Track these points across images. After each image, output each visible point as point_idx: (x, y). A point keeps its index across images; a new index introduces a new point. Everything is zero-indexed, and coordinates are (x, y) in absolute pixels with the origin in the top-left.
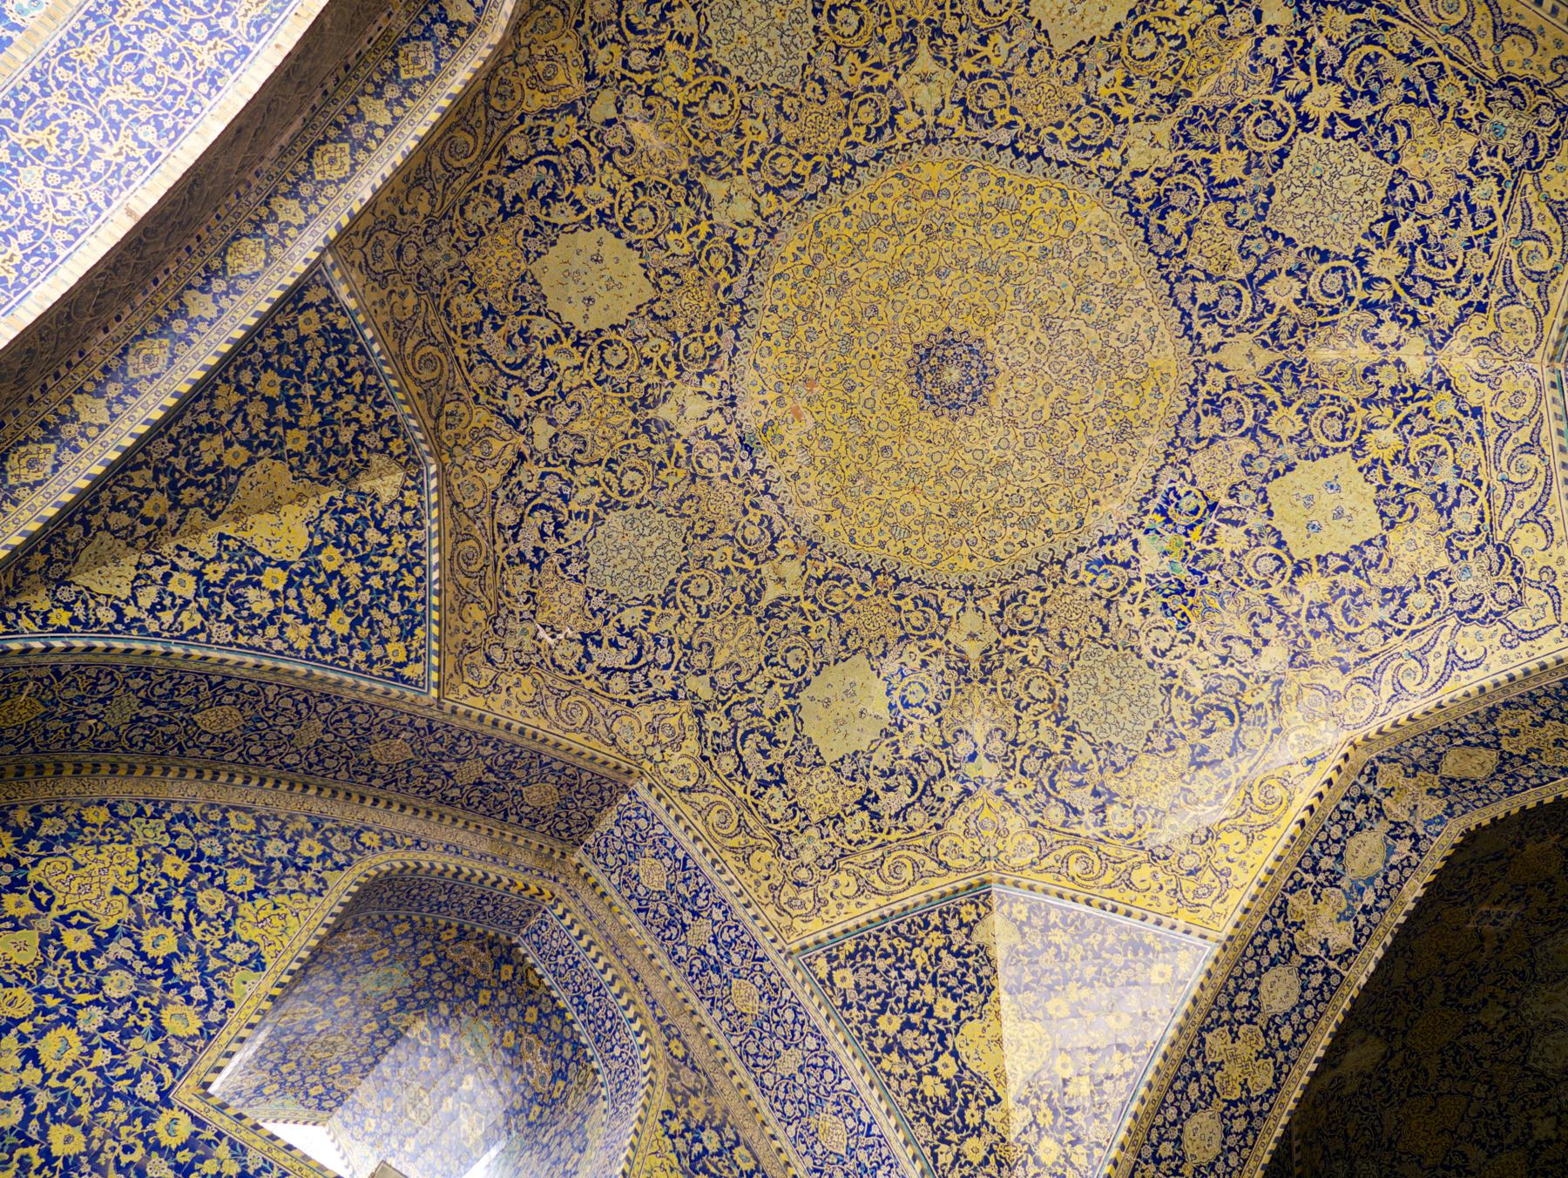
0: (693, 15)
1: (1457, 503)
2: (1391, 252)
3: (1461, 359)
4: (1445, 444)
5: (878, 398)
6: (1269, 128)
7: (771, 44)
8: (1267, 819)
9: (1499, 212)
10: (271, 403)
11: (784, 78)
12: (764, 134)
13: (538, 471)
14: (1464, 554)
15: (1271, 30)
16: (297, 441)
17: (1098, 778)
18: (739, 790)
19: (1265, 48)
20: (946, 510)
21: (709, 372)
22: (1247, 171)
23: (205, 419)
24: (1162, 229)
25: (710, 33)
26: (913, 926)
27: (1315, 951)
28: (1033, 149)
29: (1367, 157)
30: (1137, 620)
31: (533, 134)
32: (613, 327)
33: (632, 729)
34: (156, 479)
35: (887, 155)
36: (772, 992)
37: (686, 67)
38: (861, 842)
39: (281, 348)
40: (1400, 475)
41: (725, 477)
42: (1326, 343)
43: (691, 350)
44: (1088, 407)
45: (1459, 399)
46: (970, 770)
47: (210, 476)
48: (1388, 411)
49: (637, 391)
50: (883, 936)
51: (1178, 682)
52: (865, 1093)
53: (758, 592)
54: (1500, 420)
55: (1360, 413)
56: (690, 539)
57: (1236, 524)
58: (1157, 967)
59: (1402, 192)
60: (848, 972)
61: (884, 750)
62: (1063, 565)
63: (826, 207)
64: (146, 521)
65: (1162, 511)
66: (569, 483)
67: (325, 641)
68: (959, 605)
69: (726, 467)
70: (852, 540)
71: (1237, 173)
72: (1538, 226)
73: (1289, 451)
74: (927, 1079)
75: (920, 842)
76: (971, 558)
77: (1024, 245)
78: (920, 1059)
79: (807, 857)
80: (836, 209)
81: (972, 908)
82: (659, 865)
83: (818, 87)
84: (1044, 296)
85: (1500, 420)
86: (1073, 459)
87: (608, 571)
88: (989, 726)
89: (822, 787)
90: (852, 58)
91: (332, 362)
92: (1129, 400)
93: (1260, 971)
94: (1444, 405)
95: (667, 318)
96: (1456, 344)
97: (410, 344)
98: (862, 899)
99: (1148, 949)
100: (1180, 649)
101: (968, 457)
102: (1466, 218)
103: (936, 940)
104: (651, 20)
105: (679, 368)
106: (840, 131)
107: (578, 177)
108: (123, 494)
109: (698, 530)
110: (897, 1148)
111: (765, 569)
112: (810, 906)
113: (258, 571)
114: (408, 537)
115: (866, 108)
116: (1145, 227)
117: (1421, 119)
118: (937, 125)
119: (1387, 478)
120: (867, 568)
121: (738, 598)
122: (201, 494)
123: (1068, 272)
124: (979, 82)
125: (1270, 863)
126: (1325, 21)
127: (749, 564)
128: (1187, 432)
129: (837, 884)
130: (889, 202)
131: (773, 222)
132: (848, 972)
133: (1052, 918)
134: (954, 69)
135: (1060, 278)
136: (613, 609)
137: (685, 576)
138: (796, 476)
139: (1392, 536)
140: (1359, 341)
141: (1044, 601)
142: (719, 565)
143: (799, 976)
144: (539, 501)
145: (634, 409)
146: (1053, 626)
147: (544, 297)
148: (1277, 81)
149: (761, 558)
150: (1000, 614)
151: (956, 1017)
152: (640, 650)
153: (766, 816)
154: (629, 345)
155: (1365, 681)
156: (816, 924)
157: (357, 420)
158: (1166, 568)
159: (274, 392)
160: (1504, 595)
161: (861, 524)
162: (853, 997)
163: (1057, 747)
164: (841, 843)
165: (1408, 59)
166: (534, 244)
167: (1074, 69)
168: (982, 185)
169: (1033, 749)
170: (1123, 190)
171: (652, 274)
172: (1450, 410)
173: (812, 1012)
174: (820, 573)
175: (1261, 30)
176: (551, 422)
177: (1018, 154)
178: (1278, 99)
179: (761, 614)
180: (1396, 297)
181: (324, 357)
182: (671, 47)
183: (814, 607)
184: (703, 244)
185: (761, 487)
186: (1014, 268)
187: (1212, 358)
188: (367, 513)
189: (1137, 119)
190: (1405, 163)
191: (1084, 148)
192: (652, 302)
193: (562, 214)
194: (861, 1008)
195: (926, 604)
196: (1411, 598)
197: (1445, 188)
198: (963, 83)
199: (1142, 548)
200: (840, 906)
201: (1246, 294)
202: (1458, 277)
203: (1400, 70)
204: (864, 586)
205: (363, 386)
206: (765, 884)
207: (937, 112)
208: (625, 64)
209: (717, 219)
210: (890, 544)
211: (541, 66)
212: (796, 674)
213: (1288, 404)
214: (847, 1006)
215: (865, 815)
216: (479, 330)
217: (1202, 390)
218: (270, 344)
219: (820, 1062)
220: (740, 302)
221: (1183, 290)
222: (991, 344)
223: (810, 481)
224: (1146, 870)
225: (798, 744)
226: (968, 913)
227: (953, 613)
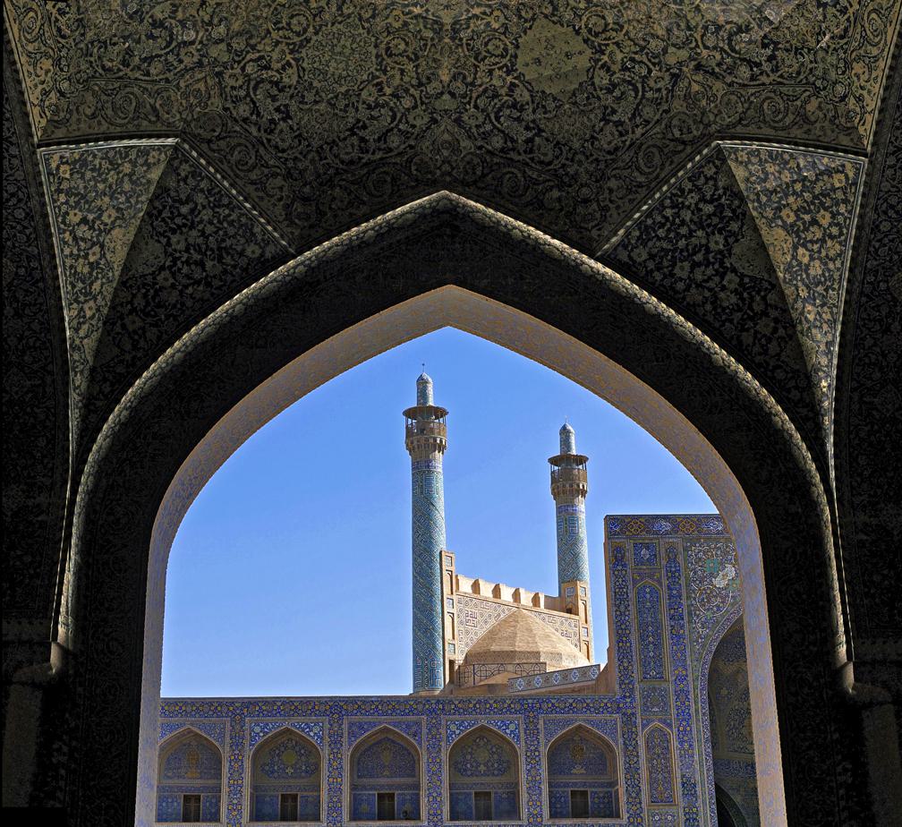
0: (363, 93)
7: (344, 47)
10: (695, 265)
13: (705, 53)
16: (718, 242)
23: (708, 307)
25: (365, 77)
31: (485, 136)
32: (578, 32)
34: (748, 330)
37: (393, 76)
39: (658, 269)
47: (745, 295)
64: (775, 330)
67: (835, 231)
91: (661, 233)
97: (642, 179)
104: (383, 111)
107: (496, 96)
108: (757, 349)
113: (800, 264)
122: (758, 298)
144: (726, 47)
154: (584, 18)
157: (696, 204)
159: (686, 265)
166: (551, 105)
171: (528, 25)
176: (665, 51)
181: (659, 239)
182: (388, 91)
192: (546, 16)
193: (523, 95)
205: (672, 208)
208: (415, 107)
211: (446, 153)
216: (619, 123)
218: (658, 276)
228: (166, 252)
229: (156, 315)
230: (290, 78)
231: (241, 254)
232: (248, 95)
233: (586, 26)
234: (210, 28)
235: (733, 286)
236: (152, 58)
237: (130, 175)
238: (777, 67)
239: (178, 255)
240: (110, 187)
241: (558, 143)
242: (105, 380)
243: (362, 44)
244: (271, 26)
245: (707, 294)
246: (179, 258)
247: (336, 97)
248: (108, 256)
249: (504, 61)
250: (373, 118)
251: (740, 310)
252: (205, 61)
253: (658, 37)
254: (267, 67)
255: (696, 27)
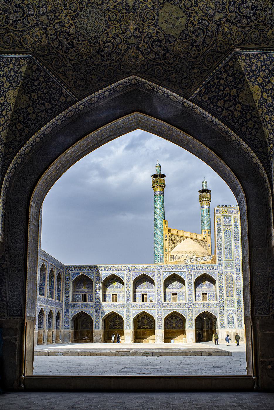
7: (92, 17)
10: (225, 102)
11: (96, 8)
13: (230, 14)
16: (234, 92)
23: (230, 117)
25: (101, 30)
31: (148, 54)
32: (181, 8)
34: (244, 126)
39: (212, 103)
47: (244, 112)
64: (254, 125)
91: (213, 89)
97: (205, 68)
104: (109, 44)
107: (151, 37)
108: (248, 133)
113: (264, 99)
122: (248, 114)
147: (183, 31)
157: (226, 77)
166: (172, 39)
171: (162, 5)
176: (214, 14)
181: (212, 92)
182: (111, 36)
188: (249, 69)
193: (161, 36)
205: (217, 79)
208: (121, 42)
211: (134, 61)
216: (197, 46)
218: (212, 106)
228: (30, 100)
229: (28, 123)
230: (73, 30)
231: (58, 100)
232: (57, 37)
233: (184, 5)
234: (39, 8)
235: (239, 109)
236: (17, 21)
237: (13, 69)
238: (257, 18)
239: (34, 101)
240: (6, 73)
241: (175, 55)
242: (10, 147)
243: (99, 16)
244: (63, 8)
245: (230, 112)
246: (35, 102)
247: (91, 38)
248: (8, 101)
249: (154, 22)
250: (105, 47)
251: (241, 118)
252: (39, 23)
253: (211, 9)
254: (63, 26)
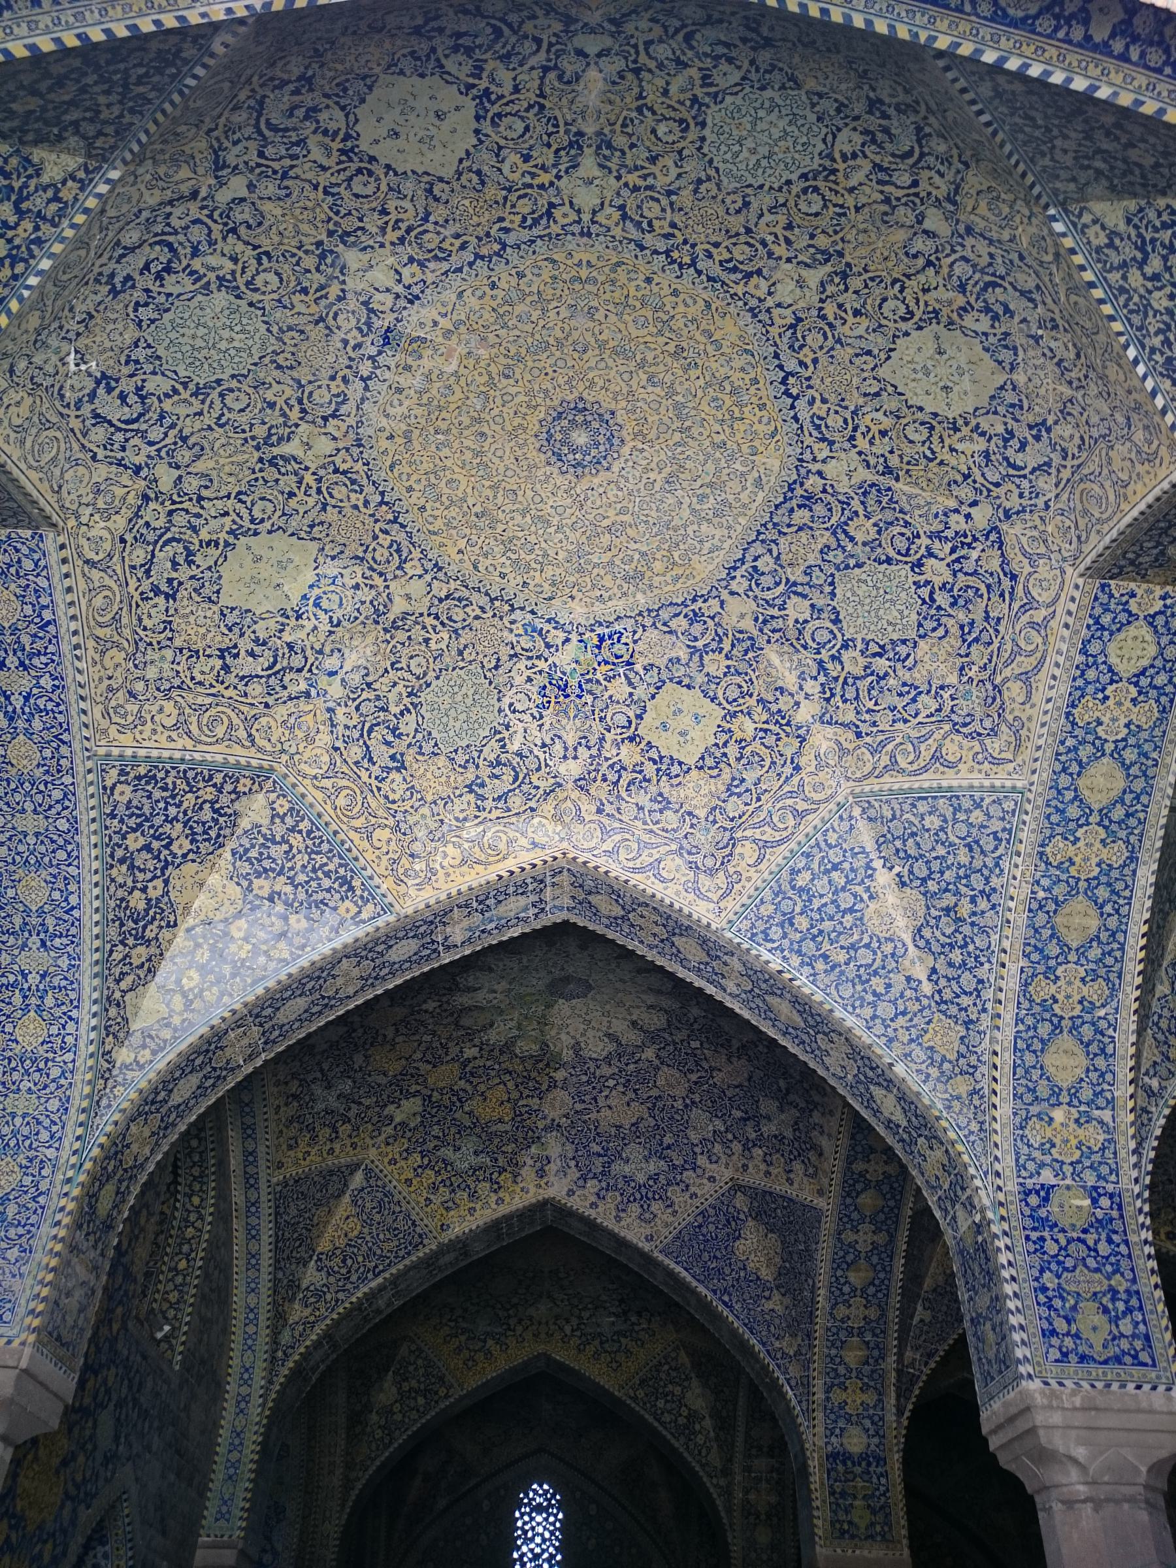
1: (739, 795)
2: (862, 661)
3: (822, 739)
4: (767, 763)
5: (517, 400)
6: (902, 544)
7: (753, 151)
8: (483, 858)
9: (920, 719)
12: (668, 180)
14: (715, 822)
15: (968, 516)
17: (403, 749)
18: (133, 583)
19: (954, 517)
20: (478, 509)
21: (421, 264)
22: (865, 544)
24: (792, 510)
26: (195, 776)
27: (440, 939)
28: (794, 391)
29: (914, 617)
30: (519, 680)
33: (80, 482)
35: (718, 285)
36: (55, 769)
37: (682, 91)
38: (200, 683)
40: (732, 751)
41: (345, 342)
42: (781, 654)
43: (426, 237)
44: (633, 546)
45: (798, 753)
46: (323, 681)
48: (765, 717)
49: (349, 224)
50: (173, 773)
51: (506, 734)
52: (85, 886)
53: (280, 439)
54: (801, 785)
55: (752, 702)
56: (267, 360)
57: (630, 684)
58: (347, 903)
59: (903, 650)
60: (128, 789)
61: (272, 624)
62: (513, 609)
63: (640, 261)
65: (601, 639)
66: (212, 243)
68: (420, 571)
69: (354, 337)
70: (392, 467)
71: (860, 537)
72: (923, 747)
73: (700, 679)
74: (137, 893)
75: (245, 709)
76: (460, 552)
77: (717, 427)
78: (140, 876)
79: (151, 673)
80: (644, 270)
81: (248, 782)
82: (17, 604)
83: (740, 204)
84: (689, 464)
85: (801, 785)
86: (589, 562)
87: (173, 335)
88: (362, 662)
89: (201, 621)
90: (783, 220)
92: (658, 566)
93: (406, 937)
94: (789, 747)
95: (437, 200)
96: (830, 731)
98: (174, 735)
99: (351, 889)
100: (527, 717)
101: (530, 493)
102: (907, 698)
103: (208, 793)
104: (708, 50)
105: (402, 240)
106: (714, 239)
109: (280, 360)
110: (86, 935)
111: (304, 426)
112: (130, 719)
114: (37, 228)
115: (747, 249)
116: (785, 500)
117: (954, 641)
118: (768, 311)
119: (725, 744)
120: (382, 494)
121: (260, 431)
123: (718, 471)
124: (822, 324)
125: (464, 888)
126: (989, 552)
127: (295, 415)
128: (665, 615)
129: (161, 710)
130: (681, 308)
131: (594, 229)
132: (128, 789)
133: (302, 826)
134: (822, 301)
135: (710, 467)
136: (148, 368)
137: (234, 384)
138: (399, 391)
139: (694, 773)
140: (796, 673)
141: (477, 618)
142: (269, 396)
143: (90, 777)
145: (330, 234)
146: (466, 637)
148: (936, 535)
149: (309, 418)
150: (441, 600)
151: (184, 856)
152: (141, 415)
153: (140, 620)
154: (384, 188)
155: (603, 828)
156: (126, 739)
158: (568, 669)
160: (709, 862)
161: (410, 463)
162: (121, 810)
163: (395, 710)
164: (185, 676)
165: (987, 618)
167: (873, 390)
168: (743, 369)
169: (378, 698)
170: (803, 471)
172: (788, 753)
173: (81, 806)
174: (343, 467)
175: (965, 509)
176: (251, 187)
177: (784, 381)
178: (924, 541)
179: (267, 457)
180: (836, 679)
183: (314, 485)
184: (531, 186)
185: (366, 374)
186: (695, 432)
187: (725, 595)
188: (17, 185)
189: (860, 453)
190: (921, 643)
191: (818, 427)
192: (441, 180)
194: (122, 821)
195: (398, 551)
196: (668, 813)
197: (918, 677)
198: (815, 313)
199: (567, 647)
200: (154, 731)
201: (781, 588)
202: (869, 711)
203: (978, 616)
204: (366, 503)
206: (106, 682)
207: (779, 305)
209: (562, 184)
210: (415, 494)
212: (252, 521)
213: (727, 658)
214: (112, 816)
215: (218, 663)
217: (699, 603)
219: (61, 842)
220: (504, 246)
221: (758, 549)
222: (626, 450)
223: (407, 403)
224: (385, 834)
225: (208, 574)
226: (244, 785)
227: (410, 573)
230: (849, 140)
232: (922, 155)
233: (378, 179)
236: (1022, 293)
244: (852, 214)
247: (783, 87)
249: (496, 109)
250: (727, 45)
254: (878, 167)
255: (224, 238)
